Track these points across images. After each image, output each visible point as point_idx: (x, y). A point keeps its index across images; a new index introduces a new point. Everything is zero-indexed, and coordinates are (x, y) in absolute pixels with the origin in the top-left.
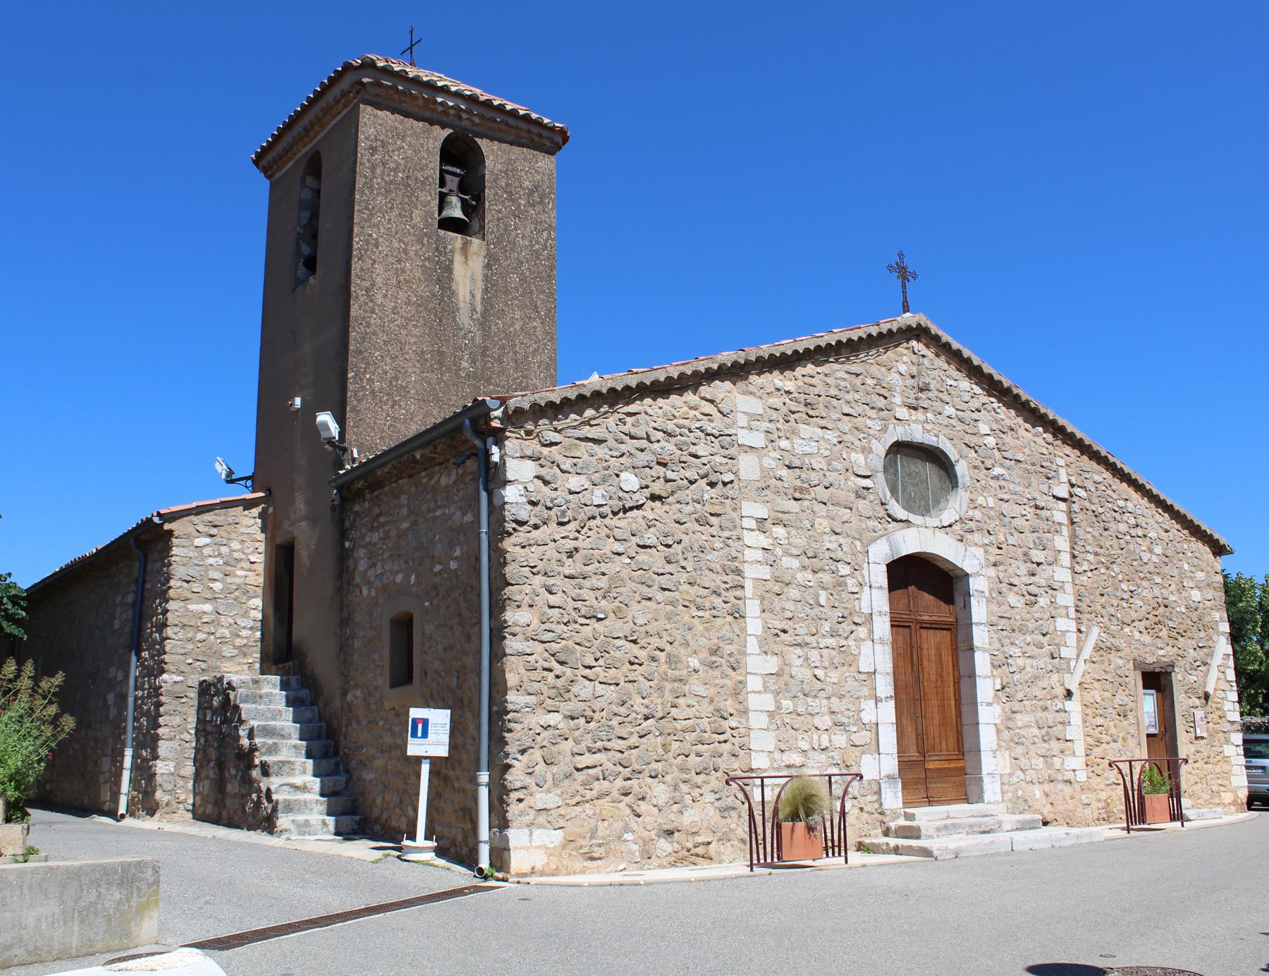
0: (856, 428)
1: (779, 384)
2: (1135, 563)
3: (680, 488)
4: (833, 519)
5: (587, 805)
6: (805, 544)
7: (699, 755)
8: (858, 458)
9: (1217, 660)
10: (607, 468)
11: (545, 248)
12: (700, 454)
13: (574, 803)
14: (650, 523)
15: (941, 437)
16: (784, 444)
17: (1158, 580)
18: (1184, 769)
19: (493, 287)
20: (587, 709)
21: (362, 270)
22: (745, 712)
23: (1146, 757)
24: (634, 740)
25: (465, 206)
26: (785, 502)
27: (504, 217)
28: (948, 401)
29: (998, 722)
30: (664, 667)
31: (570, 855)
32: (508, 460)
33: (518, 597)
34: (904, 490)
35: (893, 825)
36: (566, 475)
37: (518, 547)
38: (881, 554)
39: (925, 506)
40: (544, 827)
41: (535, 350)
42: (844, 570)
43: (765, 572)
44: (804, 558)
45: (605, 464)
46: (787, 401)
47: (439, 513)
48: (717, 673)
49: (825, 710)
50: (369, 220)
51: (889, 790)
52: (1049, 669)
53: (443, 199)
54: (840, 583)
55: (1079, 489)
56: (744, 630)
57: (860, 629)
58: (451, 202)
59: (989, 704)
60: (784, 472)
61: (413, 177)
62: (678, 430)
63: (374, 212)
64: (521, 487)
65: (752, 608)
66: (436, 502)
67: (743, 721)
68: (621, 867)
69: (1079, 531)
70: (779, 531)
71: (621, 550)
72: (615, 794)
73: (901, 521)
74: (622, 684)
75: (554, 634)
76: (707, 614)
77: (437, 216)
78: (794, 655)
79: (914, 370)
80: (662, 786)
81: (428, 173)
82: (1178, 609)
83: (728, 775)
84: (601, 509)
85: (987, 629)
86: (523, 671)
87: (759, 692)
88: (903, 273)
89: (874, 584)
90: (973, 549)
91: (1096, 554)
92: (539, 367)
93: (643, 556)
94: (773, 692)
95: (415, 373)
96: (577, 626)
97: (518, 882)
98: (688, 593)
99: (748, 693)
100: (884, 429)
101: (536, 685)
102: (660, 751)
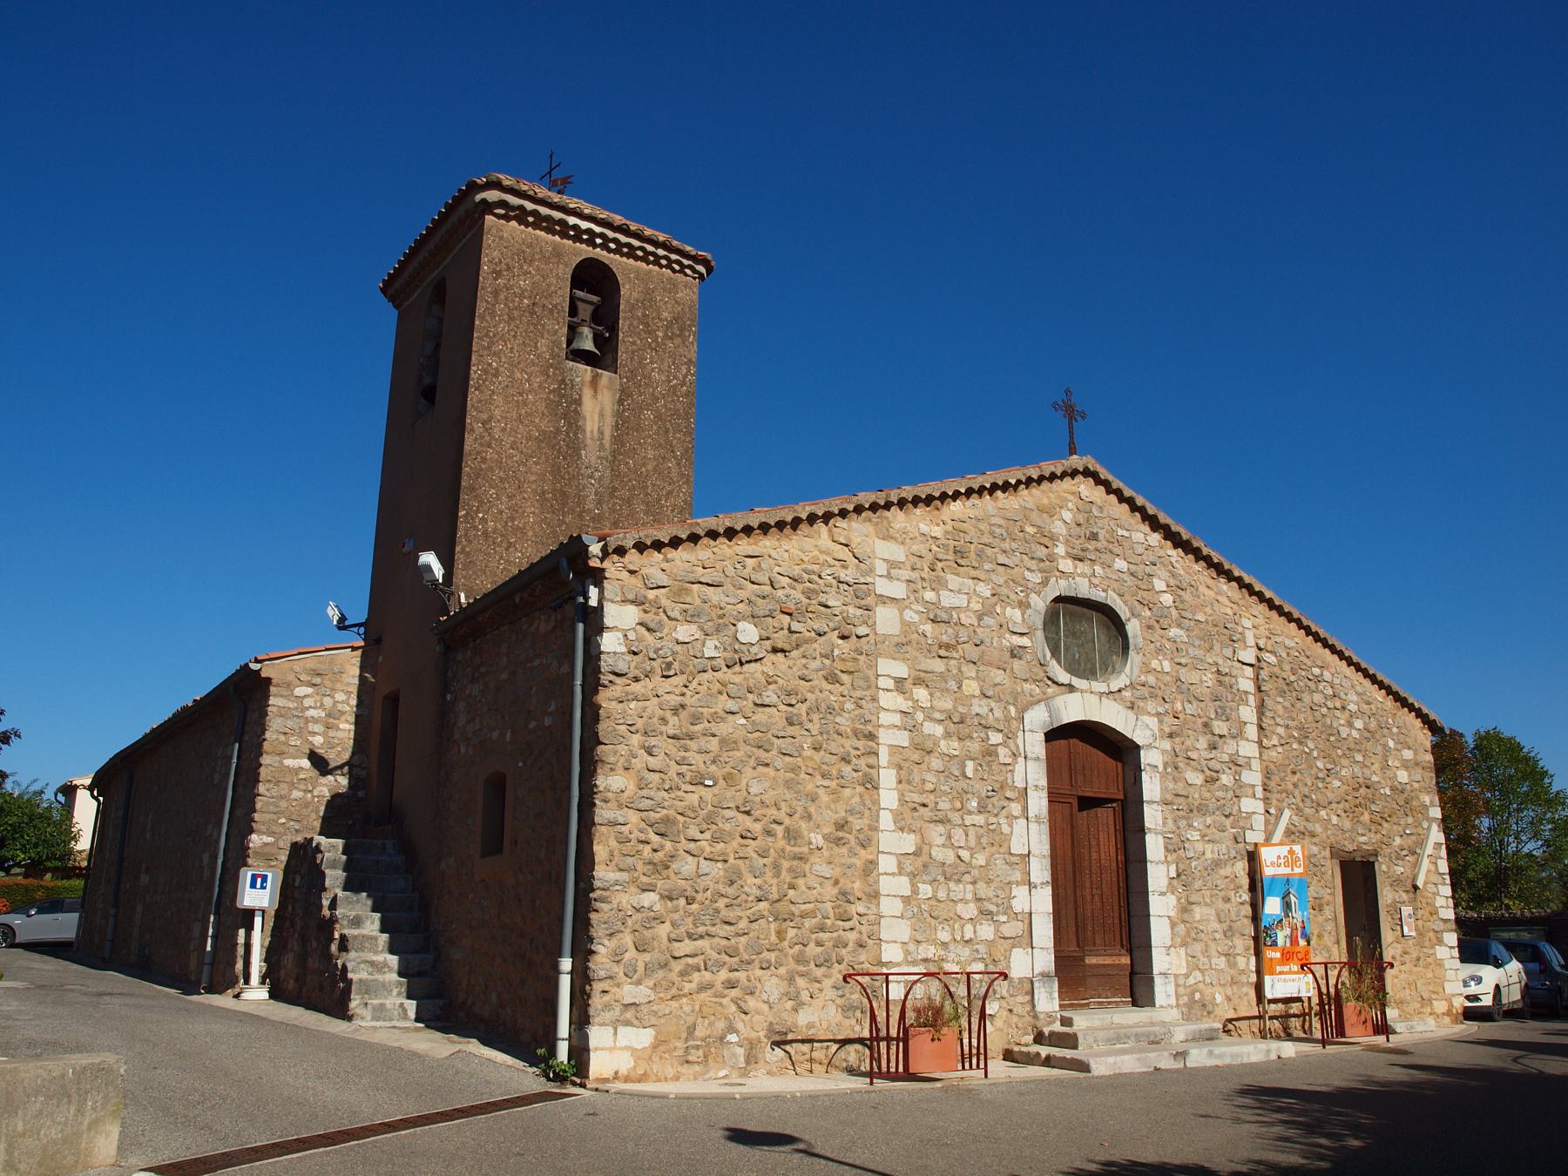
0: (1013, 580)
1: (924, 528)
2: (1332, 739)
3: (807, 641)
4: (984, 681)
6: (950, 707)
7: (819, 944)
8: (1014, 614)
9: (1429, 850)
10: (720, 617)
11: (683, 384)
12: (830, 603)
13: (669, 997)
14: (770, 680)
15: (1110, 592)
16: (929, 595)
17: (1359, 758)
18: (1389, 974)
19: (624, 425)
20: (689, 889)
21: (480, 401)
22: (875, 896)
23: (1345, 959)
24: (743, 924)
25: (597, 339)
26: (928, 660)
27: (639, 349)
28: (1119, 553)
29: (1172, 914)
30: (782, 843)
31: (661, 1058)
33: (612, 759)
35: (1046, 1030)
36: (674, 622)
37: (614, 703)
38: (1037, 719)
39: (1091, 669)
40: (632, 1025)
41: (670, 493)
42: (996, 738)
43: (903, 739)
45: (721, 612)
46: (934, 548)
47: (536, 663)
48: (844, 850)
49: (969, 896)
50: (489, 348)
51: (1043, 990)
52: (1232, 856)
54: (990, 752)
55: (1268, 654)
56: (876, 802)
57: (1013, 805)
58: (582, 333)
60: (928, 628)
62: (806, 577)
63: (495, 339)
64: (620, 635)
65: (887, 778)
67: (873, 907)
68: (722, 1073)
69: (1268, 702)
70: (921, 694)
71: (734, 709)
72: (719, 986)
73: (1062, 685)
74: (731, 860)
75: (653, 802)
76: (833, 784)
77: (565, 346)
78: (936, 834)
80: (775, 980)
81: (556, 300)
82: (1382, 791)
83: (854, 969)
84: (714, 662)
85: (1160, 808)
86: (613, 843)
87: (893, 874)
88: (1071, 412)
89: (1029, 755)
90: (1146, 719)
91: (1287, 727)
92: (673, 511)
93: (761, 716)
94: (908, 875)
95: (533, 513)
96: (680, 793)
97: (597, 1090)
98: (811, 759)
99: (880, 874)
100: (1045, 583)
101: (630, 860)
102: (774, 938)
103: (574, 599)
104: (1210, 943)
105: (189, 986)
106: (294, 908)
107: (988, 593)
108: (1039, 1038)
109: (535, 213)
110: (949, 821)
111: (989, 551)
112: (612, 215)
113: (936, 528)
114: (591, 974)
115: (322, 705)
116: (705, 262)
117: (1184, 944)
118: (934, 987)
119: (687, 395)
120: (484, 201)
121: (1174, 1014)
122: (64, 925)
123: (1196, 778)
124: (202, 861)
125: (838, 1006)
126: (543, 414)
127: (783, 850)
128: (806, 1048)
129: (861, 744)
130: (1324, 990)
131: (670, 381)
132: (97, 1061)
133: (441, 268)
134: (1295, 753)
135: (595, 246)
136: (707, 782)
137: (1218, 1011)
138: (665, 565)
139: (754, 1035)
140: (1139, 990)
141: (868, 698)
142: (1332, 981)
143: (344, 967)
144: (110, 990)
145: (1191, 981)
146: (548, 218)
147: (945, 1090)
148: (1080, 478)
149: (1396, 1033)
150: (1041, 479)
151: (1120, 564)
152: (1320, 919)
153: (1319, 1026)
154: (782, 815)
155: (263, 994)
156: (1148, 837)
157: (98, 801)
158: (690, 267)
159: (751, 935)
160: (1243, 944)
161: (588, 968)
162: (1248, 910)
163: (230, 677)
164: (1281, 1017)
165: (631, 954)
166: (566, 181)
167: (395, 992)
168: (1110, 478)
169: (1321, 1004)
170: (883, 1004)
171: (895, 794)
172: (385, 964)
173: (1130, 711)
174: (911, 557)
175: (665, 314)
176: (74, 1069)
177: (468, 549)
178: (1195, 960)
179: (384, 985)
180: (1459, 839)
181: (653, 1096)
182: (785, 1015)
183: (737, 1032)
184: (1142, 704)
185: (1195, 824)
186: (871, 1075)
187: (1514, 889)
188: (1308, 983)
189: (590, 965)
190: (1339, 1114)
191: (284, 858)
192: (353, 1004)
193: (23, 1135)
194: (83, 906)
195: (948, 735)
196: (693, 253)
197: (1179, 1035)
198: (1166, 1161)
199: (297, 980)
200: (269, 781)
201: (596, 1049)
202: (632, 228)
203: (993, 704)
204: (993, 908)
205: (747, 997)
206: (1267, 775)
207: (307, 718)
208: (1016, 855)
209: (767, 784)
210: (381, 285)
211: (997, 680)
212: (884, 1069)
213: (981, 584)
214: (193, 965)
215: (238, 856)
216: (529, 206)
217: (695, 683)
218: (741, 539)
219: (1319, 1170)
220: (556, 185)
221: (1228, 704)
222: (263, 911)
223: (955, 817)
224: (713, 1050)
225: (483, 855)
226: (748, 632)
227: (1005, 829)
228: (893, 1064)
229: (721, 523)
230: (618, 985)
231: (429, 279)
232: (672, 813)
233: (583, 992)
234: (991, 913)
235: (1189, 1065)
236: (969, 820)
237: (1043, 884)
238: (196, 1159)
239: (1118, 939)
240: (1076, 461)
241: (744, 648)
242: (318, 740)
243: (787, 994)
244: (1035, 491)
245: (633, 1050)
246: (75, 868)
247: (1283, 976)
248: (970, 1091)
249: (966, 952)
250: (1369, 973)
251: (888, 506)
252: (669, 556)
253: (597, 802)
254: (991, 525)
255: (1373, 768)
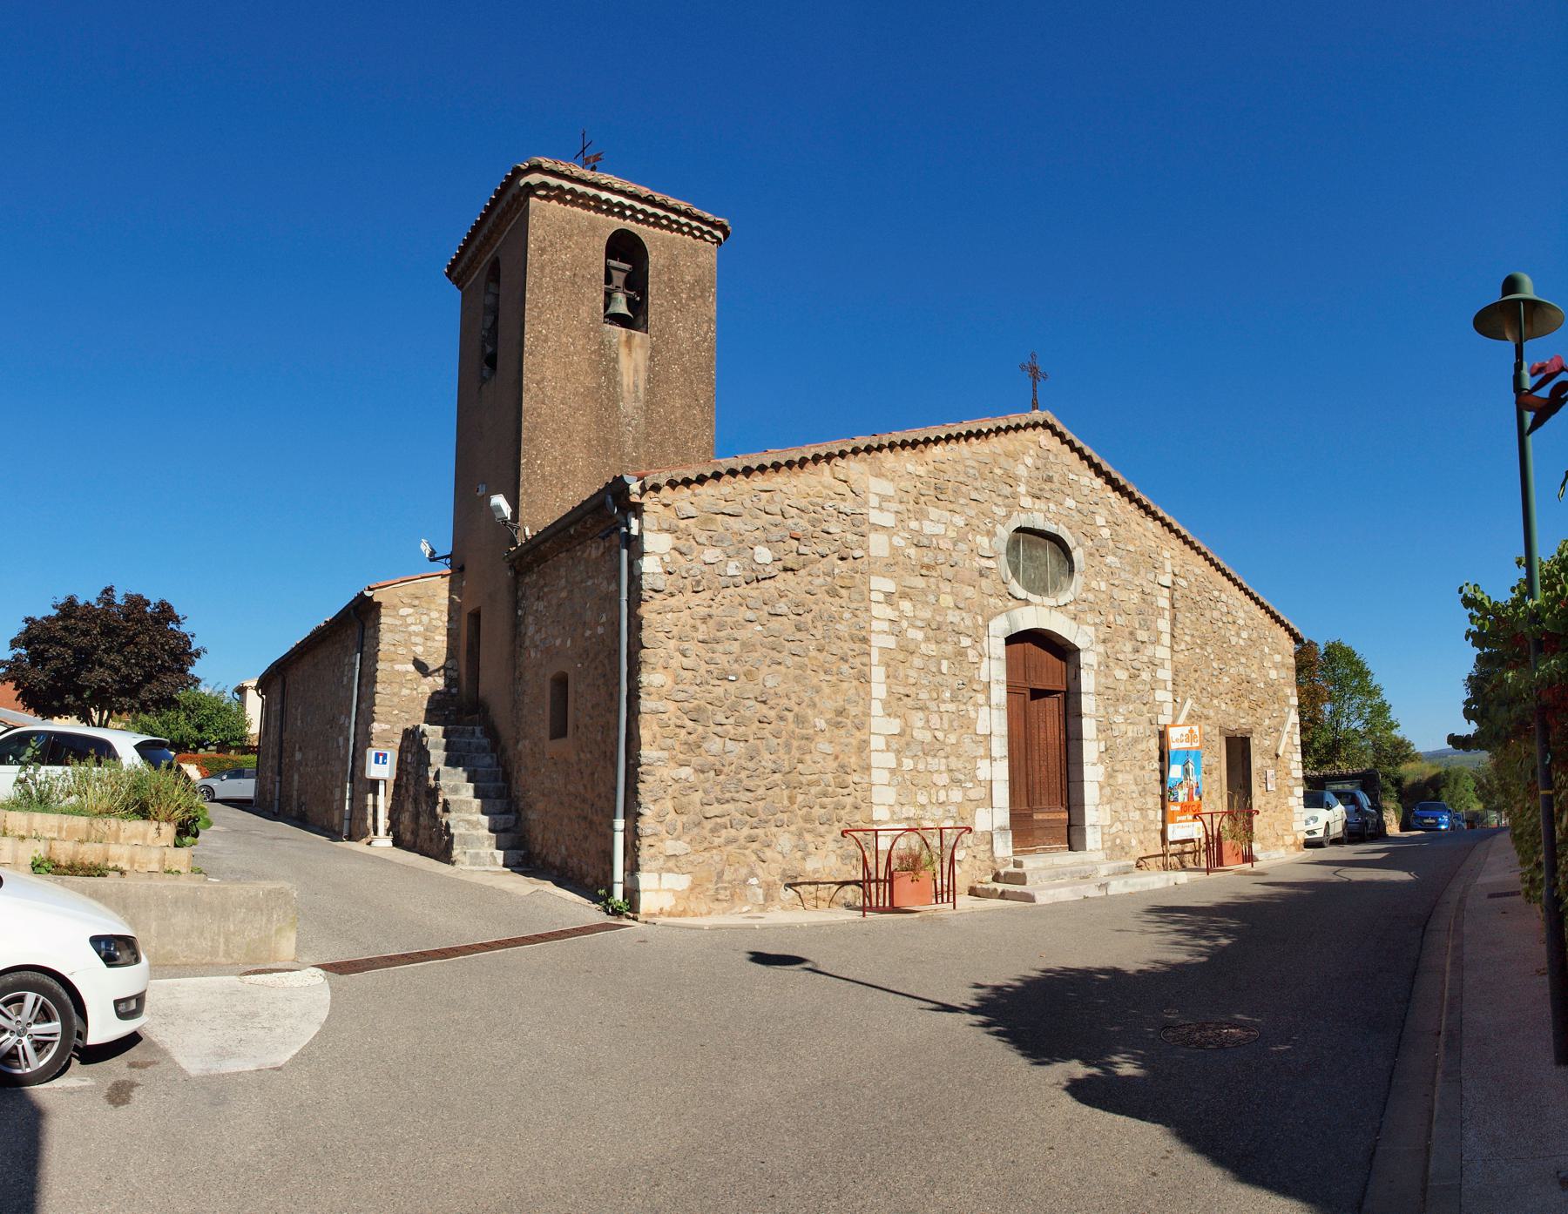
0: (982, 513)
1: (910, 468)
5: (714, 851)
6: (929, 616)
8: (983, 541)
9: (1288, 728)
10: (741, 542)
12: (831, 531)
13: (702, 849)
14: (782, 594)
15: (1061, 525)
16: (914, 525)
18: (1256, 818)
20: (718, 763)
24: (761, 791)
26: (912, 578)
28: (1069, 493)
29: (1101, 779)
30: (792, 726)
31: (697, 898)
32: (645, 533)
33: (653, 660)
34: (1024, 571)
36: (702, 547)
38: (1000, 627)
39: (1043, 587)
40: (673, 872)
42: (966, 642)
43: (891, 642)
44: (928, 629)
46: (919, 485)
47: (589, 583)
48: (842, 732)
49: (943, 768)
50: (539, 317)
53: (609, 296)
54: (961, 653)
56: (869, 693)
57: (979, 695)
58: (616, 299)
59: (1094, 764)
60: (912, 551)
61: (580, 275)
62: (811, 508)
64: (658, 558)
65: (878, 674)
66: (588, 573)
68: (745, 909)
70: (906, 605)
71: (752, 618)
72: (742, 841)
73: (1020, 599)
74: (751, 740)
75: (687, 695)
76: (834, 679)
77: (602, 311)
78: (917, 719)
79: (1039, 463)
81: (593, 270)
83: (850, 826)
84: (735, 580)
85: (1094, 698)
86: (655, 728)
87: (882, 751)
88: (1034, 372)
89: (993, 656)
90: (1086, 628)
91: (1192, 636)
93: (775, 624)
94: (895, 751)
96: (710, 687)
97: (646, 922)
98: (816, 658)
100: (1008, 516)
101: (669, 742)
102: (786, 802)
103: (618, 529)
105: (335, 835)
106: (407, 779)
107: (962, 524)
108: (996, 878)
109: (572, 191)
110: (927, 708)
111: (964, 488)
112: (639, 187)
113: (920, 468)
114: (640, 832)
115: (421, 621)
116: (722, 228)
117: (1109, 802)
118: (914, 840)
119: (708, 350)
120: (528, 184)
121: (1101, 855)
122: (245, 788)
123: (1122, 675)
124: (338, 743)
125: (837, 855)
126: (587, 372)
127: (793, 732)
128: (812, 888)
129: (856, 646)
130: (1210, 833)
131: (693, 338)
132: (278, 887)
133: (495, 249)
134: (1198, 656)
135: (625, 217)
136: (731, 678)
137: (1133, 852)
138: (693, 499)
139: (770, 878)
140: (1074, 838)
141: (862, 609)
142: (1216, 827)
143: (448, 824)
144: (281, 836)
146: (584, 195)
147: (922, 919)
148: (1040, 429)
149: (1257, 860)
150: (1008, 429)
151: (1070, 503)
152: (1210, 780)
153: (1205, 860)
154: (792, 704)
155: (388, 842)
156: (1084, 721)
157: (263, 698)
158: (709, 233)
159: (768, 800)
160: (1153, 801)
161: (637, 827)
162: (1158, 775)
163: (351, 602)
164: (1179, 854)
165: (672, 816)
166: (597, 158)
167: (486, 843)
168: (1065, 431)
169: (1207, 843)
170: (874, 853)
171: (884, 687)
172: (478, 822)
173: (1073, 622)
174: (899, 492)
175: (688, 278)
176: (263, 891)
177: (529, 491)
179: (478, 838)
180: (1310, 720)
181: (691, 928)
182: (795, 863)
183: (757, 876)
184: (1082, 616)
185: (1121, 710)
186: (864, 909)
187: (1343, 754)
188: (1199, 828)
189: (639, 824)
190: (1215, 922)
191: (398, 741)
192: (455, 853)
193: (234, 934)
194: (258, 773)
195: (927, 639)
196: (712, 219)
197: (1103, 871)
198: (1089, 965)
199: (412, 833)
200: (384, 682)
201: (645, 891)
202: (657, 199)
203: (964, 614)
205: (766, 849)
206: (1176, 672)
207: (410, 633)
208: (981, 735)
209: (780, 679)
210: (446, 270)
211: (968, 595)
212: (874, 904)
214: (336, 820)
215: (365, 739)
216: (567, 185)
217: (720, 596)
218: (757, 477)
219: (1199, 964)
220: (589, 163)
221: (1149, 617)
222: (385, 781)
223: (932, 706)
224: (737, 890)
225: (553, 737)
226: (764, 555)
227: (972, 714)
228: (881, 900)
229: (739, 463)
230: (662, 841)
231: (485, 261)
232: (702, 703)
233: (634, 845)
236: (943, 707)
237: (1001, 757)
238: (349, 962)
239: (1060, 801)
240: (1038, 415)
241: (760, 567)
242: (419, 650)
243: (796, 846)
244: (1003, 438)
245: (675, 892)
246: (249, 747)
247: (1181, 824)
248: (941, 919)
249: (939, 812)
250: (1242, 817)
251: (880, 448)
252: (697, 491)
253: (641, 695)
255: (1253, 668)
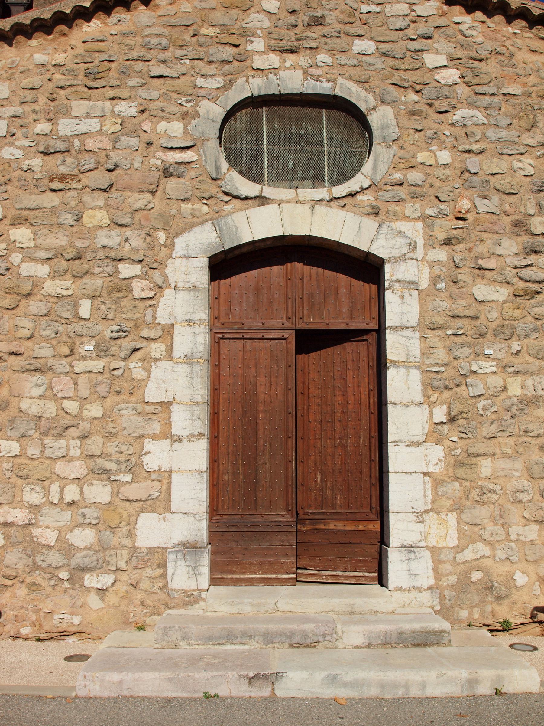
1: (39, 58)
60: (37, 162)
104: (508, 506)
145: (468, 555)
178: (476, 529)
204: (112, 466)
208: (154, 404)
213: (123, 102)
234: (106, 472)
235: (280, 693)
237: (192, 436)
254: (143, 37)
